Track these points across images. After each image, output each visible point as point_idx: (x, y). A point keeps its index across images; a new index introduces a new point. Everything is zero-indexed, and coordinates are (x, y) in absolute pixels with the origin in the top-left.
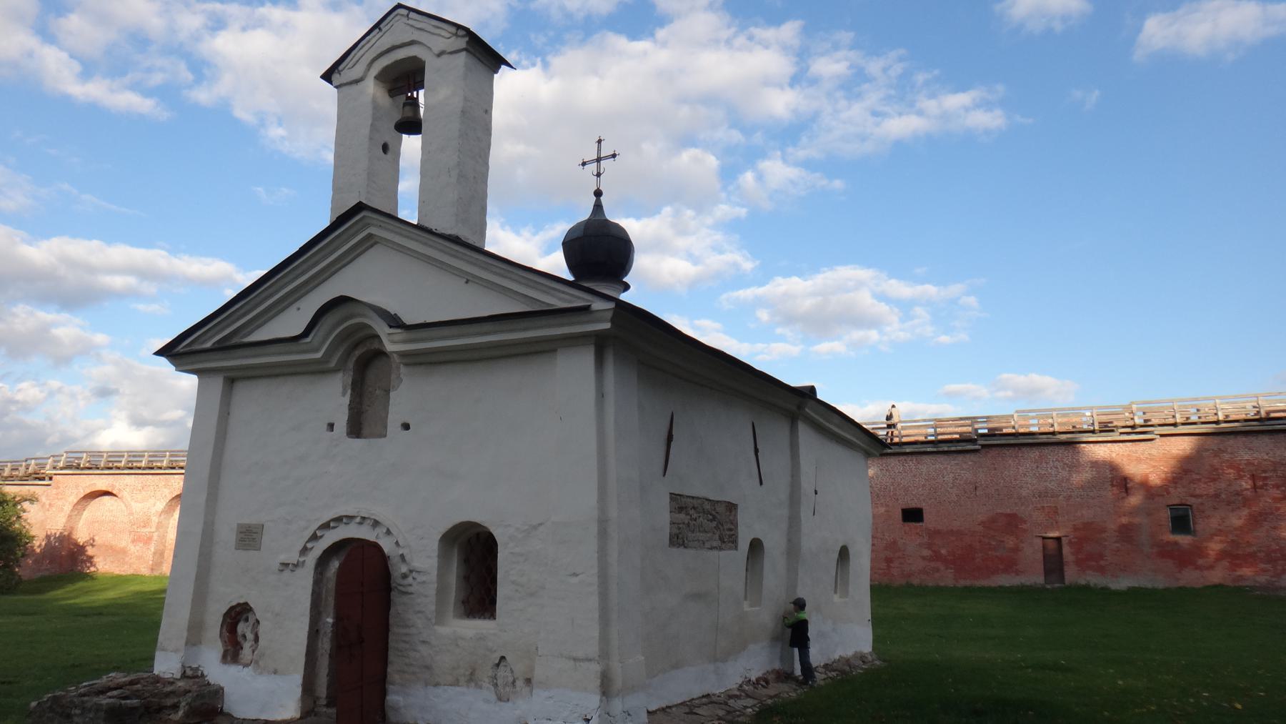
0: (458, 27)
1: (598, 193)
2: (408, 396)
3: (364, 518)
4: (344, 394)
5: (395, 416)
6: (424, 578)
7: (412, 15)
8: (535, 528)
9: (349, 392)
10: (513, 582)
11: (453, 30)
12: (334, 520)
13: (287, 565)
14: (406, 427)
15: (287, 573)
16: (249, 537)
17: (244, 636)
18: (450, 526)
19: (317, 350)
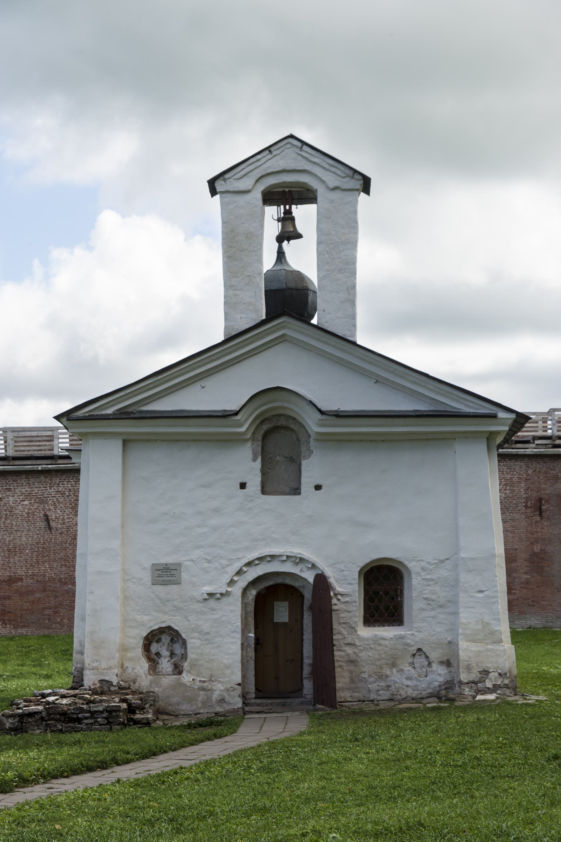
0: (355, 171)
3: (287, 556)
4: (254, 460)
5: (308, 479)
6: (347, 599)
7: (305, 148)
8: (442, 561)
9: (259, 459)
10: (426, 599)
11: (350, 173)
13: (211, 595)
14: (318, 487)
16: (166, 574)
17: (158, 654)
18: (368, 561)
19: (241, 426)
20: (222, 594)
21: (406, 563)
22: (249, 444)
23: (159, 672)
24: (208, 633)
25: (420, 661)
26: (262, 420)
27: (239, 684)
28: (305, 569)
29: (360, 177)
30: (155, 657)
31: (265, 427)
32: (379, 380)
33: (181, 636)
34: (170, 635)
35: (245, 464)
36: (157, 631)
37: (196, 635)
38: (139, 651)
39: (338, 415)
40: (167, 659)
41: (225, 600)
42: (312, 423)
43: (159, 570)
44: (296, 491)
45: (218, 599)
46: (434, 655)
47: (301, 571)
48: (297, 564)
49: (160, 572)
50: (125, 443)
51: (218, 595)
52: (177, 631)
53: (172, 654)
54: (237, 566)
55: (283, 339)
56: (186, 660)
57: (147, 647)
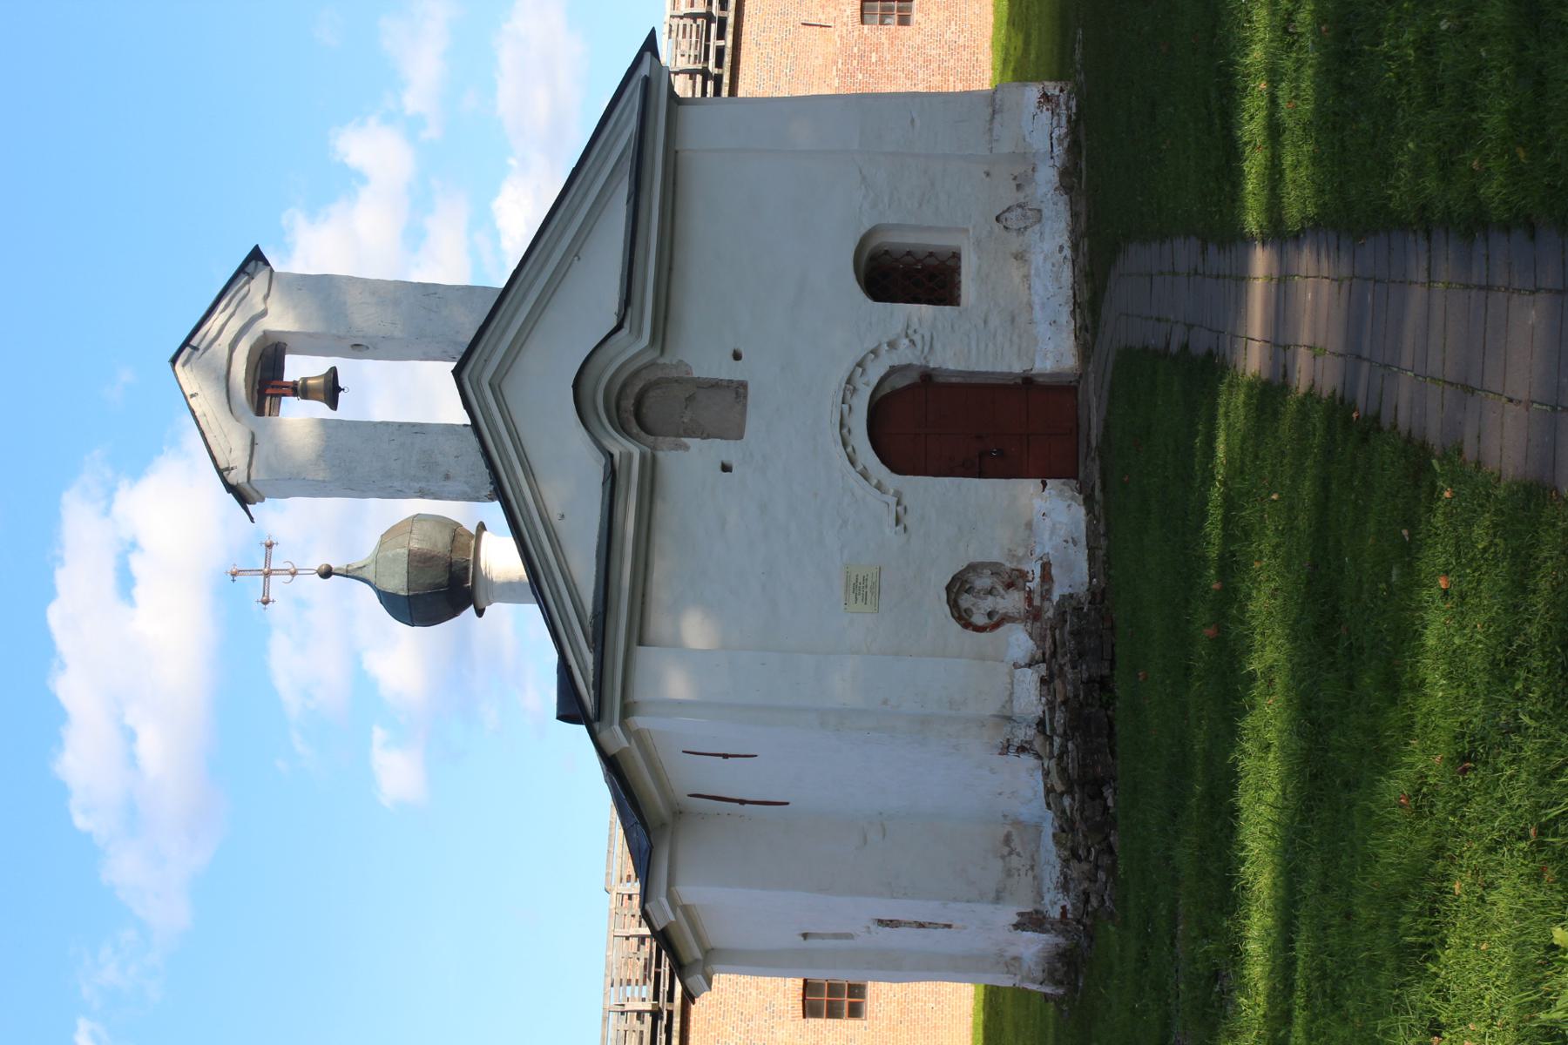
0: (241, 270)
1: (327, 573)
2: (701, 355)
4: (686, 448)
5: (724, 370)
6: (915, 320)
7: (194, 342)
8: (864, 178)
12: (845, 445)
13: (898, 522)
14: (737, 356)
15: (908, 520)
17: (990, 615)
19: (630, 456)
20: (898, 503)
21: (863, 231)
22: (660, 454)
25: (1013, 219)
26: (623, 430)
27: (1045, 485)
28: (865, 379)
29: (253, 264)
31: (636, 429)
32: (574, 251)
34: (958, 593)
35: (689, 464)
38: (983, 635)
39: (627, 301)
40: (999, 599)
41: (905, 502)
42: (634, 346)
44: (739, 390)
46: (1009, 196)
47: (867, 384)
48: (855, 389)
50: (641, 643)
53: (990, 592)
54: (853, 477)
55: (496, 388)
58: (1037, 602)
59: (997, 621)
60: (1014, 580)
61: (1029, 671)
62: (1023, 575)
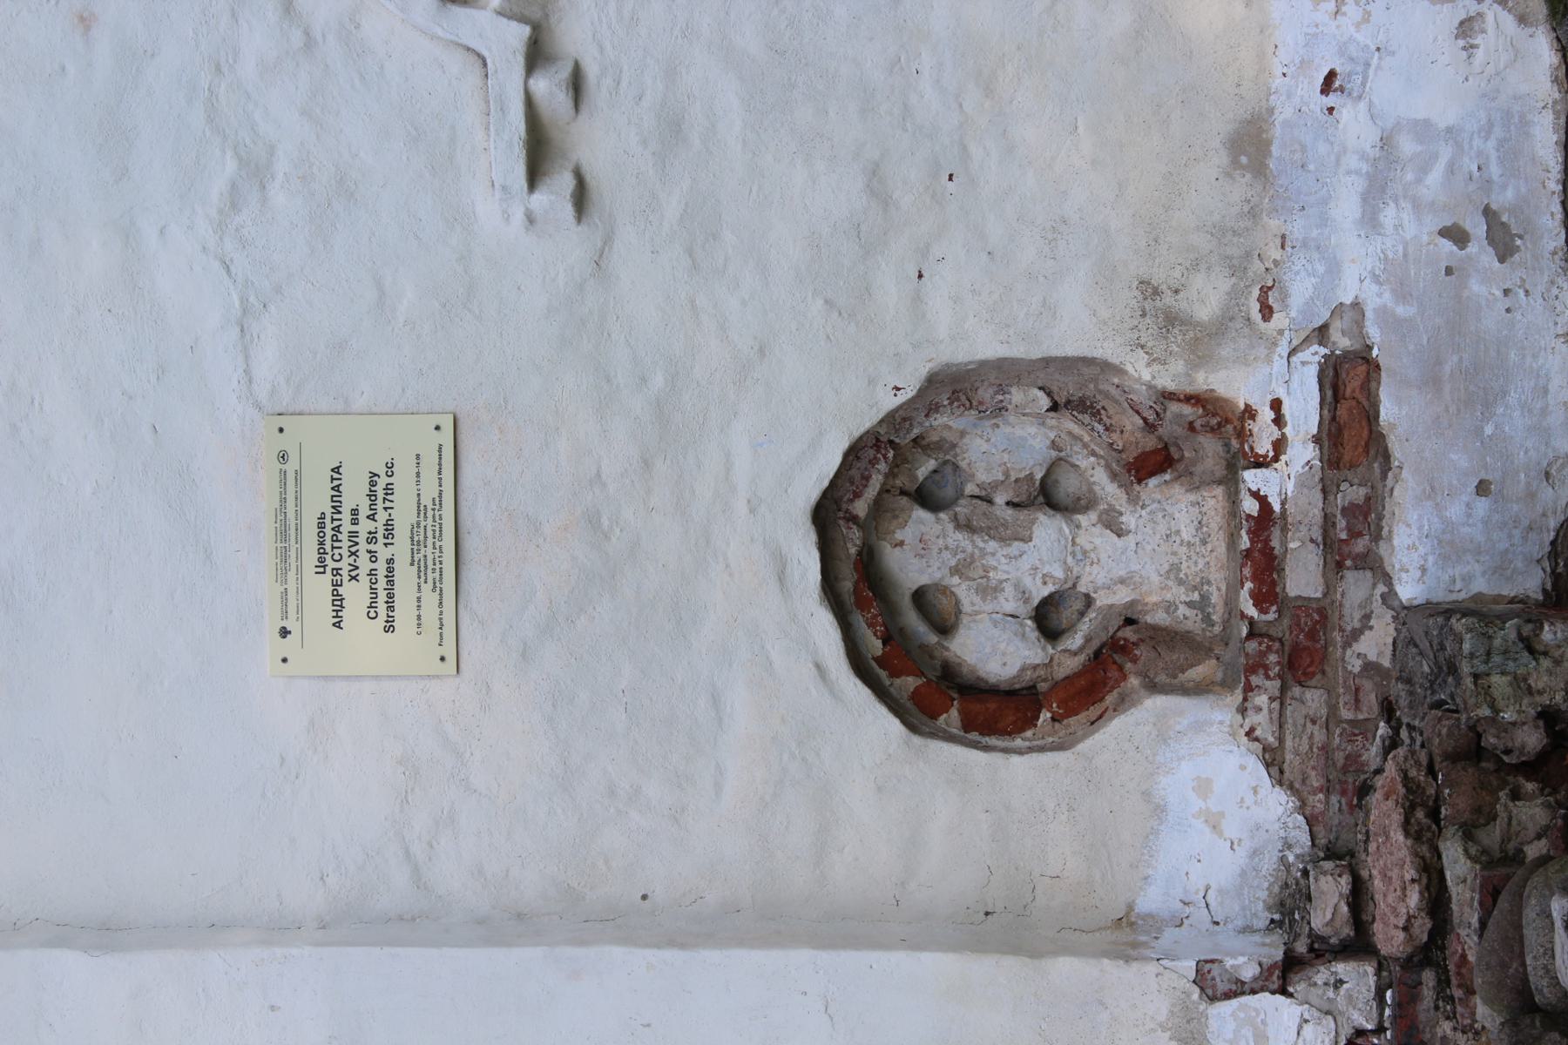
13: (539, 153)
15: (601, 142)
17: (1047, 619)
20: (537, 55)
23: (1202, 605)
24: (876, 183)
30: (1075, 641)
33: (896, 419)
36: (859, 621)
37: (890, 289)
38: (1018, 775)
41: (577, 35)
43: (338, 601)
45: (576, 84)
49: (356, 595)
51: (549, 87)
52: (853, 453)
53: (1046, 495)
56: (1105, 366)
57: (1000, 714)
58: (1303, 577)
59: (1098, 669)
60: (1185, 440)
61: (1279, 1012)
62: (1223, 421)
